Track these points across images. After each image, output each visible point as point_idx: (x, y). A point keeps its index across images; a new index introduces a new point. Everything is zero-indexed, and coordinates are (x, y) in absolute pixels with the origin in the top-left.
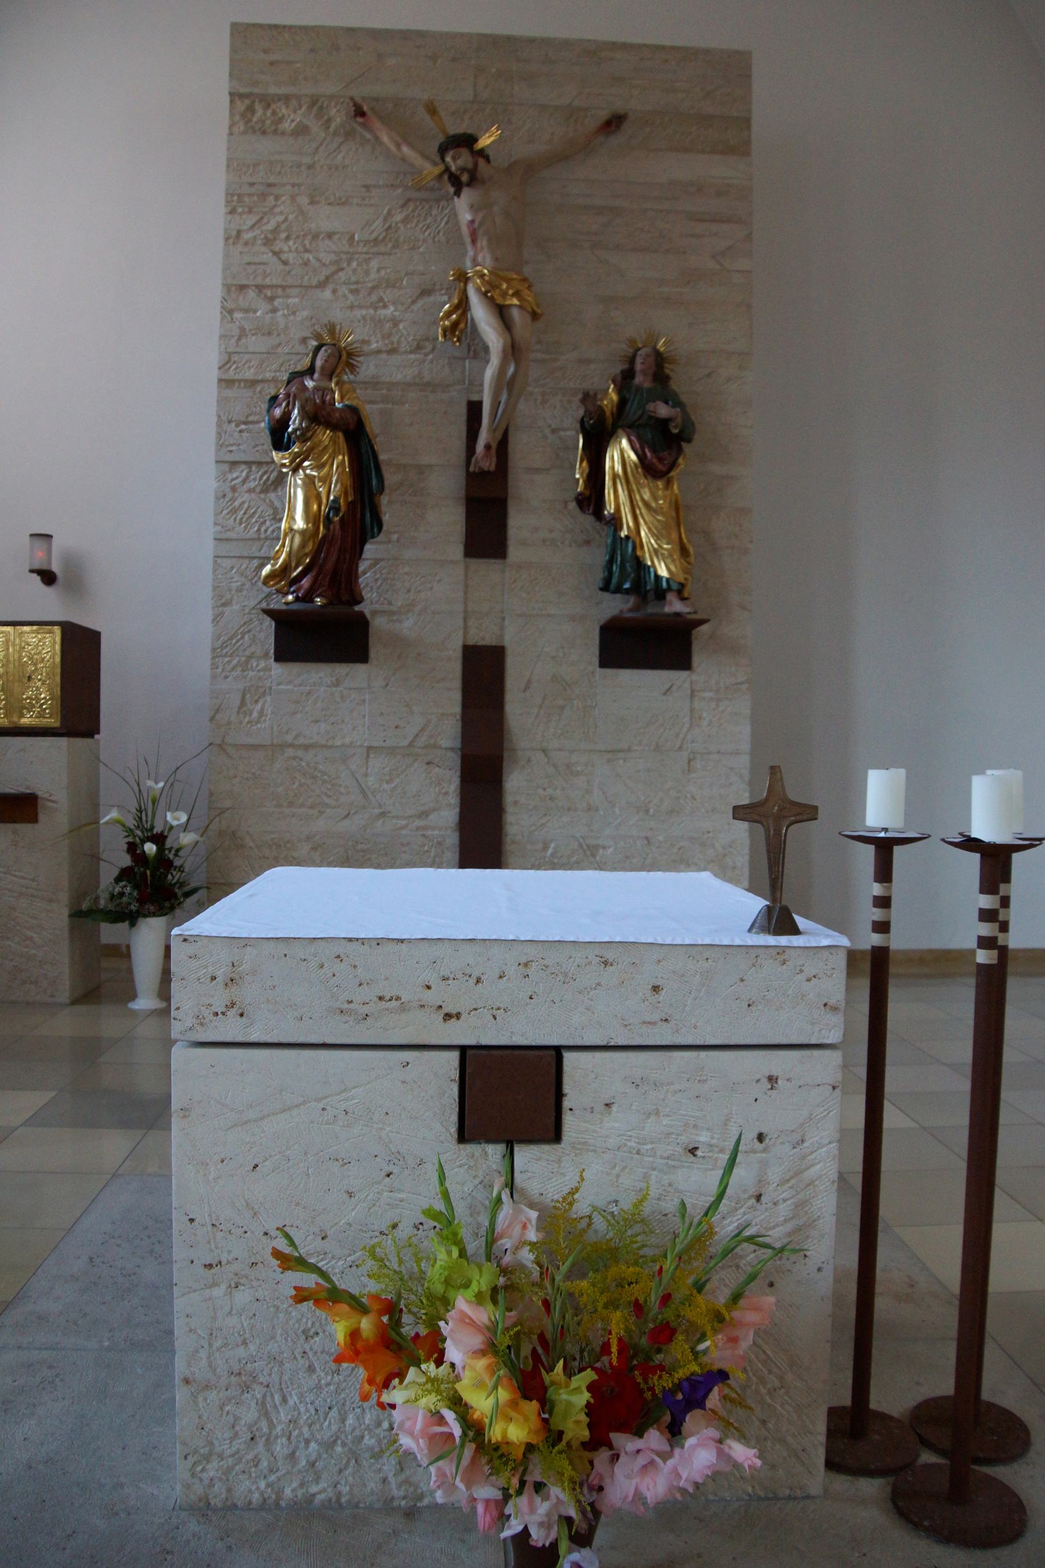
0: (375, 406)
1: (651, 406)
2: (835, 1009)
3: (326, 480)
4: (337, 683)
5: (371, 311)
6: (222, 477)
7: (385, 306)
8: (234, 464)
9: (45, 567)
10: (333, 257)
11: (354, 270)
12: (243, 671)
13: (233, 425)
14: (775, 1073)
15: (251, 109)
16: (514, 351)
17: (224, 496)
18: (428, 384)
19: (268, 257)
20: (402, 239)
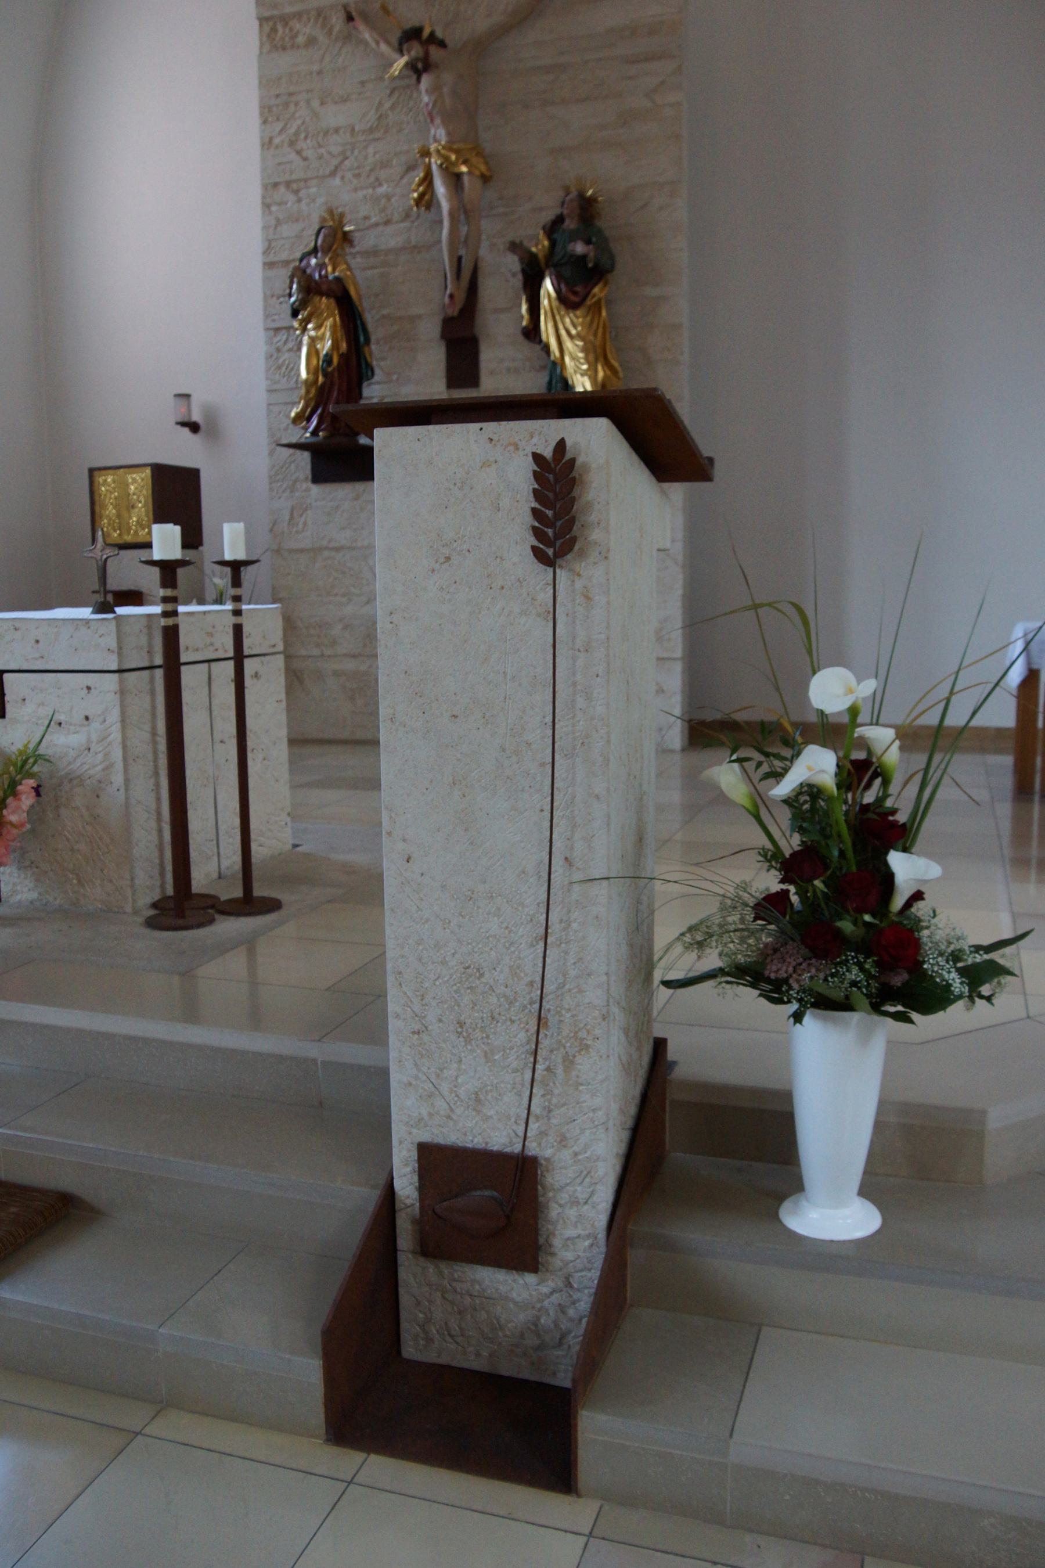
0: (376, 271)
1: (570, 247)
2: (113, 652)
4: (357, 498)
5: (370, 191)
6: (269, 342)
7: (380, 185)
8: (277, 330)
9: (186, 420)
10: (340, 149)
11: (356, 158)
12: (292, 492)
13: (275, 298)
14: (89, 684)
15: (274, 30)
17: (271, 356)
18: (415, 247)
19: (293, 156)
20: (391, 124)
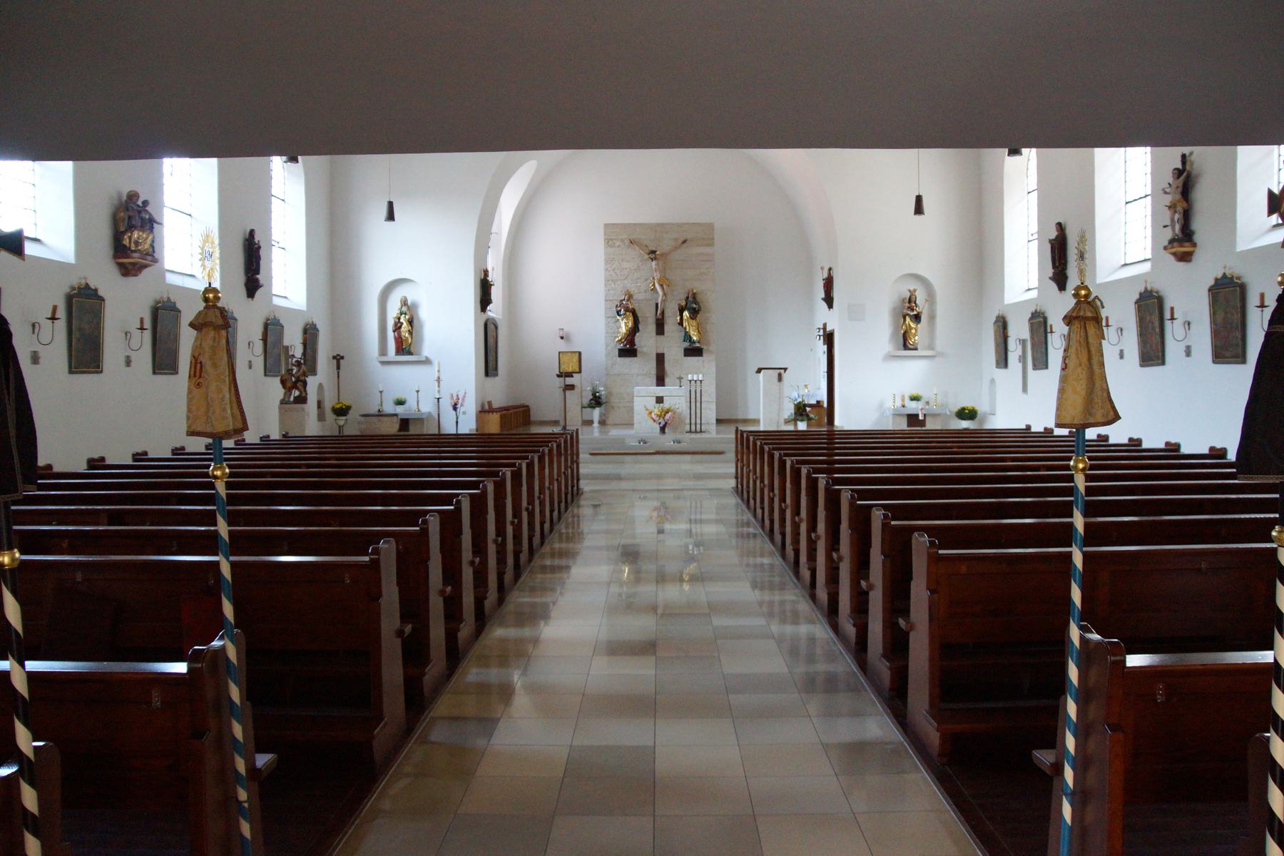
3: (628, 322)
8: (609, 317)
15: (608, 242)
16: (665, 294)
